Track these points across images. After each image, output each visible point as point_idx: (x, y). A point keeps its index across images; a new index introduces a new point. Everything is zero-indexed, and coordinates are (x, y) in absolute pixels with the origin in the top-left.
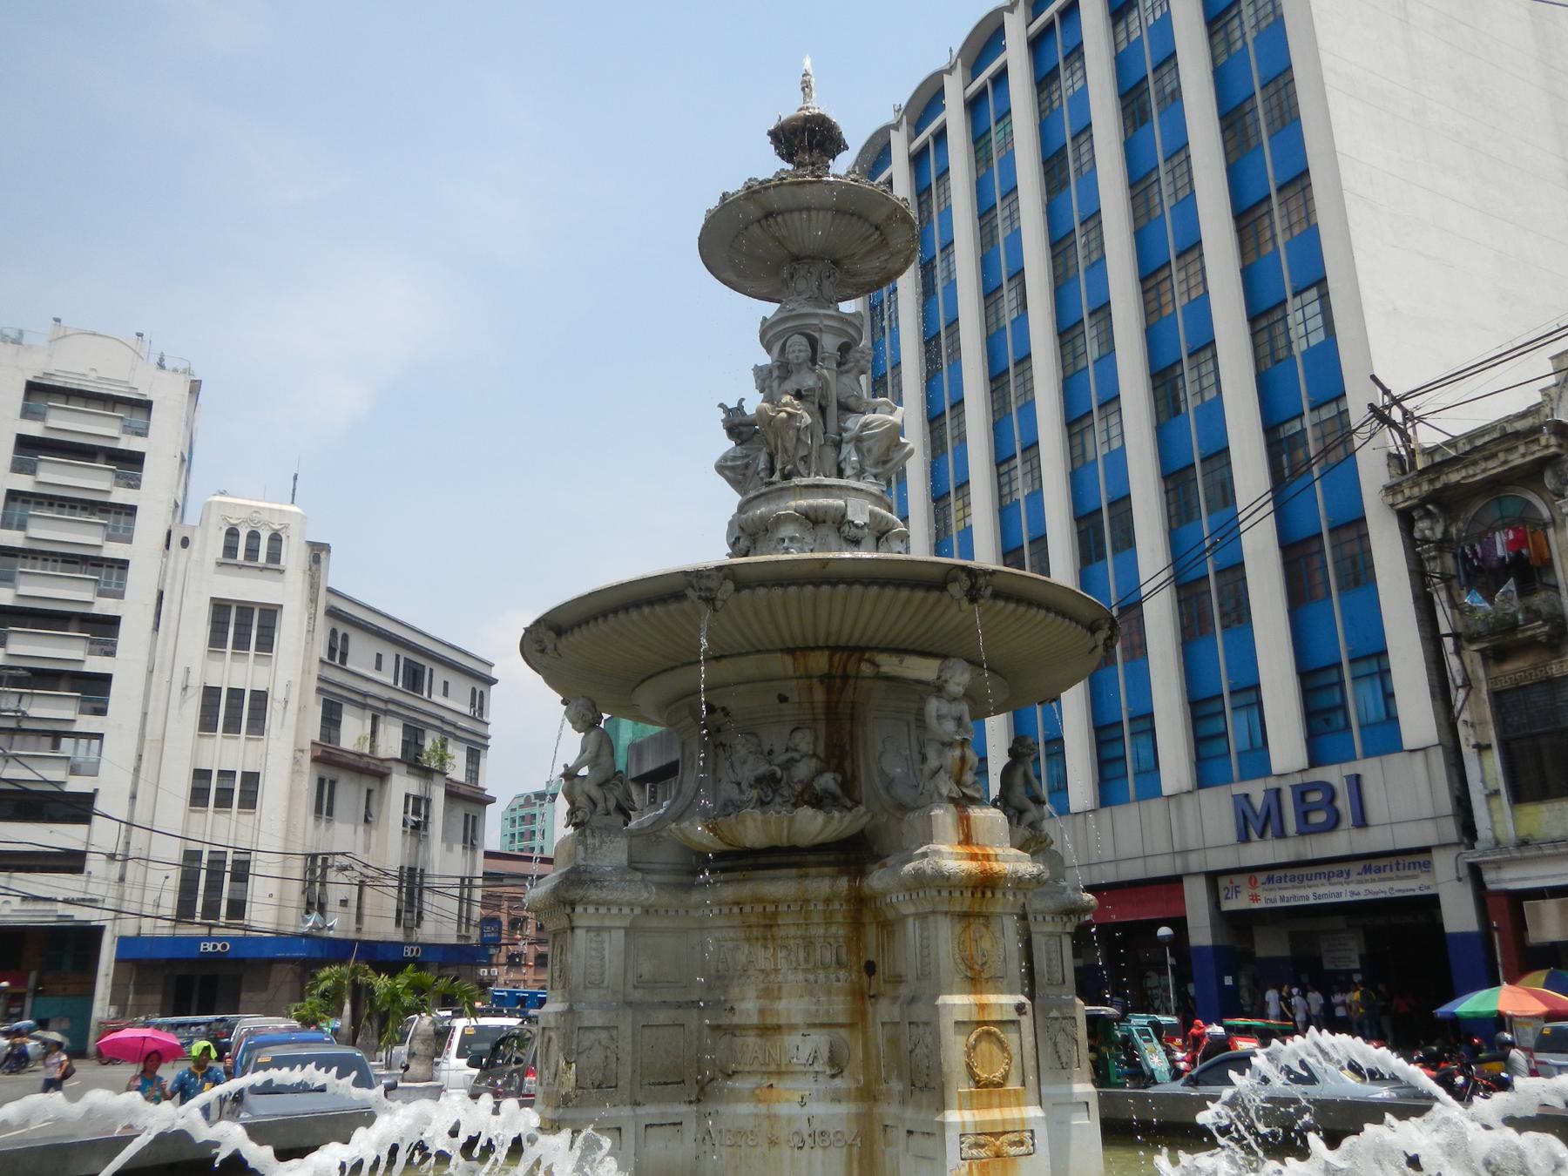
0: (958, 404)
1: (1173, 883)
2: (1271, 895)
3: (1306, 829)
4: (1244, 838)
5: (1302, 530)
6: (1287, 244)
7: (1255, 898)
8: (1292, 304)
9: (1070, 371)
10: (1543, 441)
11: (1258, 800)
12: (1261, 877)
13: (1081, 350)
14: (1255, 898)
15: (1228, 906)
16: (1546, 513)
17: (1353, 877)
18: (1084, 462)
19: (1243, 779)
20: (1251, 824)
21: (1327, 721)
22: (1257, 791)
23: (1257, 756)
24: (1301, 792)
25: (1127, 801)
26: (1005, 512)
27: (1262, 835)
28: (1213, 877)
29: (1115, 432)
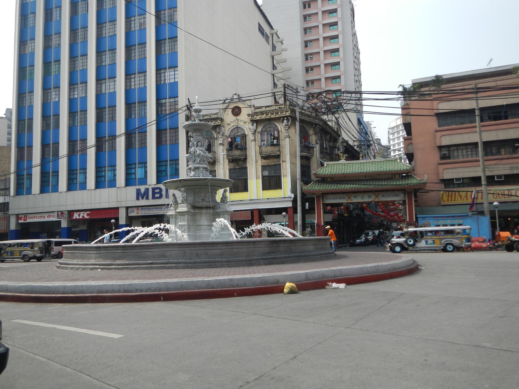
0: (58, 61)
1: (117, 209)
2: (142, 213)
3: (154, 198)
4: (138, 199)
5: (163, 127)
6: (168, 54)
7: (138, 213)
8: (167, 70)
9: (99, 65)
11: (143, 191)
12: (140, 208)
13: (104, 60)
14: (138, 213)
15: (130, 215)
16: (216, 137)
17: (163, 209)
18: (101, 93)
19: (138, 185)
20: (139, 195)
21: (161, 174)
22: (143, 188)
23: (144, 181)
24: (154, 189)
25: (105, 188)
26: (72, 102)
27: (142, 198)
28: (127, 208)
29: (112, 87)
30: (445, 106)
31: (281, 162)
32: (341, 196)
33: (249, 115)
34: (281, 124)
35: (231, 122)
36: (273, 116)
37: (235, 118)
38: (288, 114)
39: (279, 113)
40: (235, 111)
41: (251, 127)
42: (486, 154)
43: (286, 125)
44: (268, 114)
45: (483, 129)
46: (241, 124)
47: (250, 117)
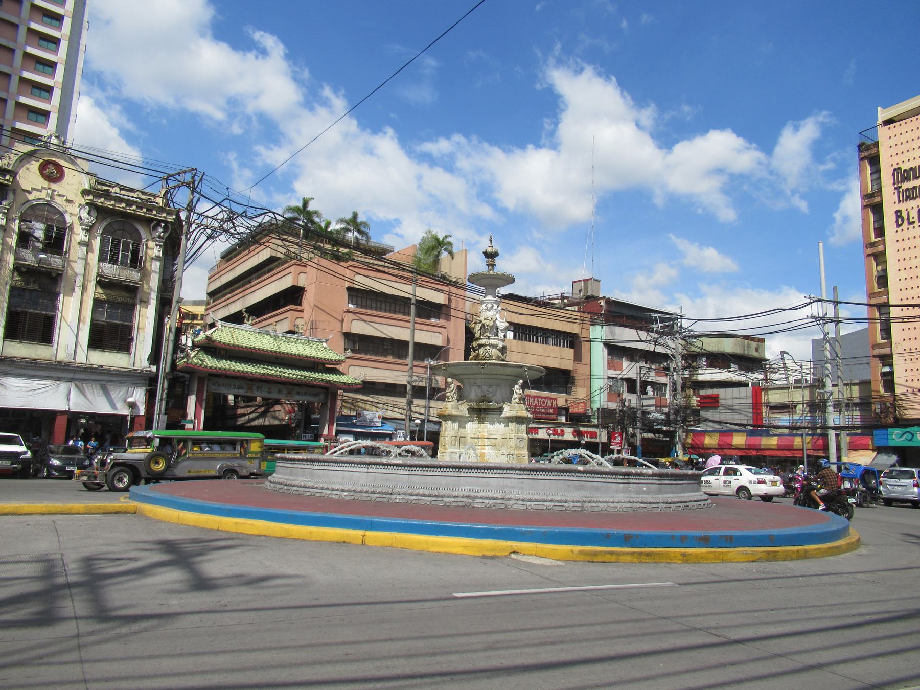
10: (7, 177)
30: (364, 281)
31: (138, 301)
32: (237, 383)
33: (85, 192)
34: (147, 230)
35: (33, 189)
36: (140, 213)
37: (45, 184)
38: (171, 218)
39: (154, 212)
40: (47, 171)
41: (84, 214)
42: (416, 358)
43: (159, 237)
44: (131, 206)
45: (417, 326)
46: (59, 202)
47: (91, 197)
